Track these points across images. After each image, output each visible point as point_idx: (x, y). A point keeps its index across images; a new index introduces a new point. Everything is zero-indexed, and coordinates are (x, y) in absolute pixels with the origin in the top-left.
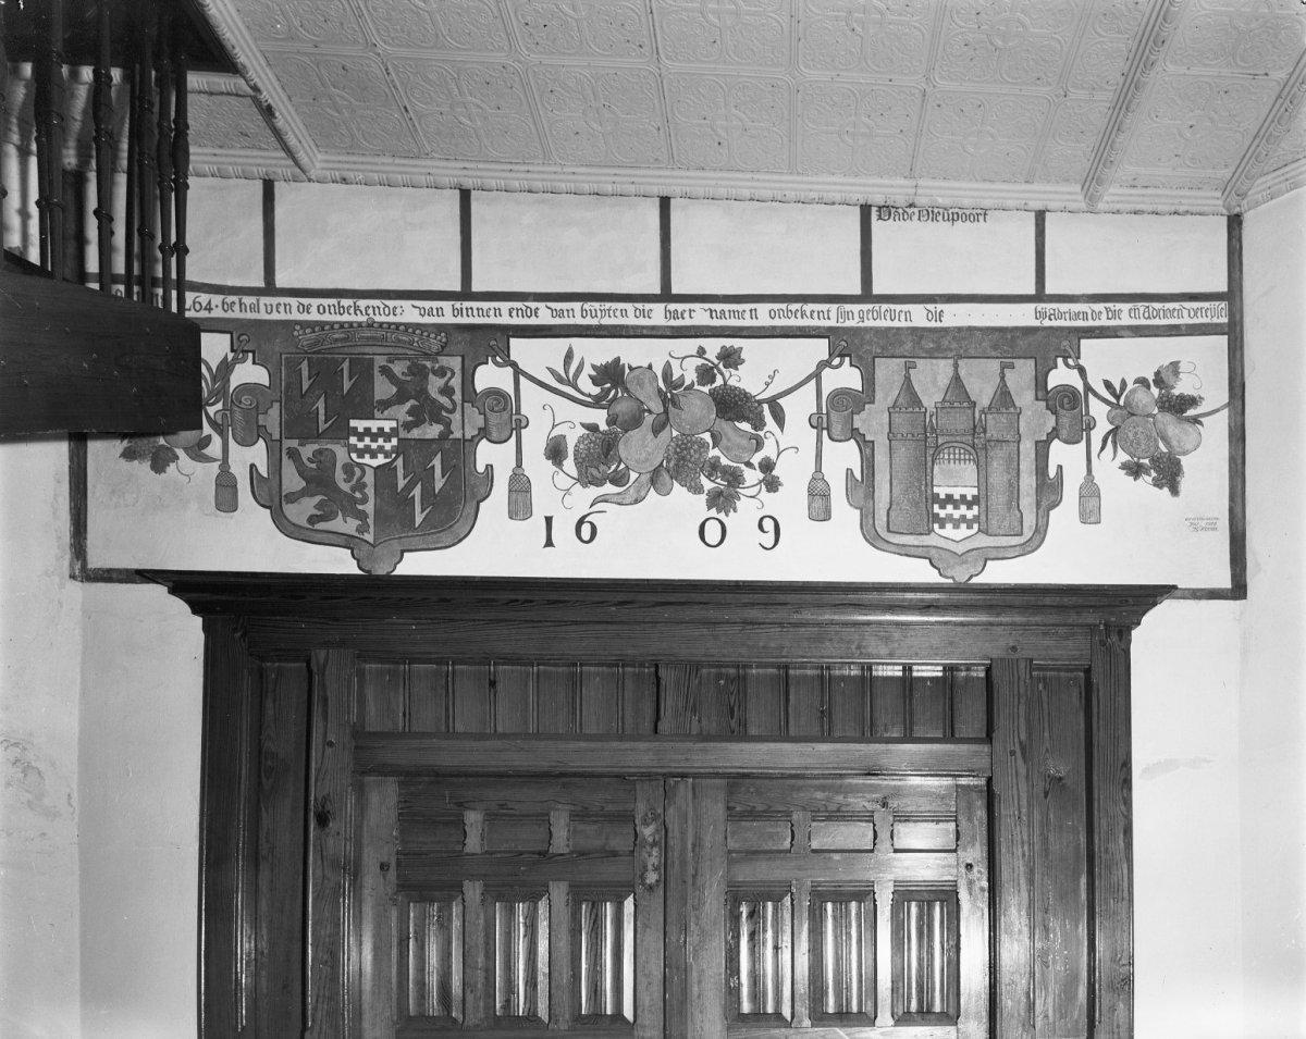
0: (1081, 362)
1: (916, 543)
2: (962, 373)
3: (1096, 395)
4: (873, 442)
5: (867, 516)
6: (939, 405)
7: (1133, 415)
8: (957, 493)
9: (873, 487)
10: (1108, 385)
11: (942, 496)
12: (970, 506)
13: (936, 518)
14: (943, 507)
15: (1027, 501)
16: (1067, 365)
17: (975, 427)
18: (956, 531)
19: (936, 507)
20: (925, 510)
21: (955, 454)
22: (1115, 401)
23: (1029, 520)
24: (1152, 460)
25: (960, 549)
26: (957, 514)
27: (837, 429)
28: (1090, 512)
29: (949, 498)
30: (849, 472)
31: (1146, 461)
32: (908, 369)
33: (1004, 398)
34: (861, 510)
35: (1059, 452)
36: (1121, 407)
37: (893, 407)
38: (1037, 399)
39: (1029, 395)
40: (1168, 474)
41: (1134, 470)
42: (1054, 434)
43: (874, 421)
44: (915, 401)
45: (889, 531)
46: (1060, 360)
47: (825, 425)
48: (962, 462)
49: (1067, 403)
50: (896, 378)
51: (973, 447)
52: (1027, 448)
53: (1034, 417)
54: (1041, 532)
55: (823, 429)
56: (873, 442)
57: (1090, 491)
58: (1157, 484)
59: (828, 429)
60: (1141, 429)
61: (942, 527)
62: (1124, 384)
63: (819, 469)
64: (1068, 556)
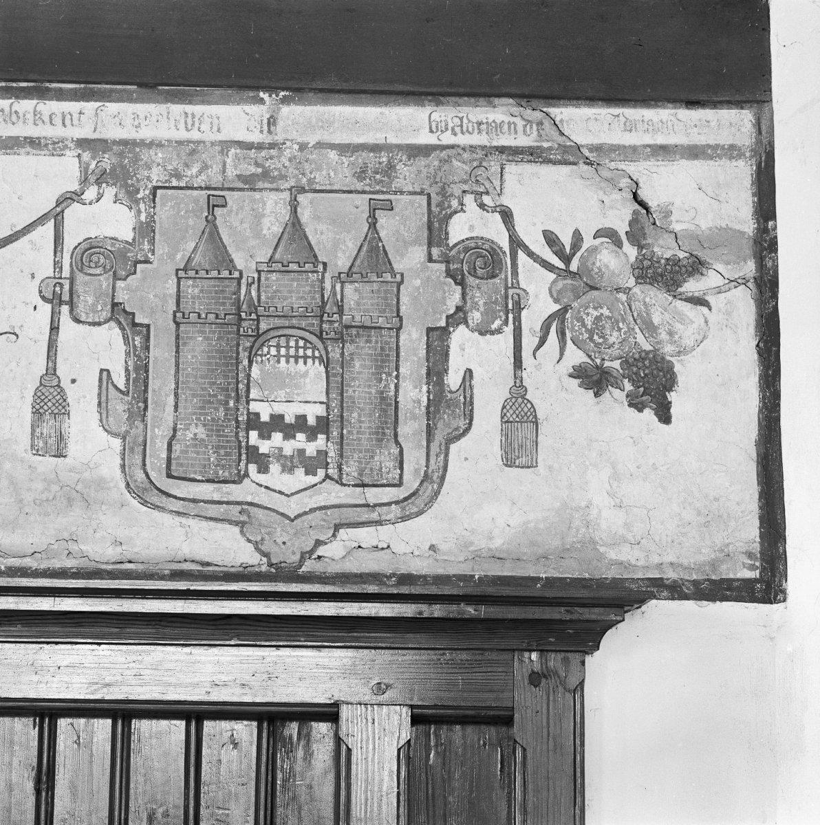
0: (506, 201)
1: (216, 497)
2: (305, 215)
3: (531, 254)
4: (148, 326)
5: (132, 450)
6: (264, 267)
7: (593, 288)
8: (290, 413)
9: (145, 401)
10: (551, 239)
11: (265, 418)
12: (312, 435)
13: (253, 455)
14: (265, 436)
15: (411, 428)
16: (482, 206)
17: (324, 303)
18: (286, 476)
19: (254, 435)
20: (238, 441)
21: (288, 347)
22: (561, 265)
23: (414, 459)
24: (626, 363)
25: (293, 507)
26: (289, 447)
27: (86, 300)
28: (519, 446)
29: (277, 422)
30: (105, 374)
31: (616, 364)
32: (211, 207)
33: (374, 258)
34: (124, 438)
35: (465, 349)
36: (574, 275)
37: (185, 270)
38: (430, 260)
39: (418, 254)
40: (653, 386)
41: (594, 379)
42: (459, 316)
43: (152, 293)
44: (223, 259)
45: (169, 476)
46: (469, 200)
47: (66, 297)
48: (301, 361)
49: (481, 264)
50: (191, 222)
51: (320, 337)
52: (413, 340)
53: (422, 286)
54: (434, 479)
55: (61, 303)
56: (148, 326)
57: (520, 416)
58: (636, 404)
59: (71, 303)
60: (605, 311)
61: (264, 469)
62: (577, 238)
63: (51, 371)
64: (476, 519)
